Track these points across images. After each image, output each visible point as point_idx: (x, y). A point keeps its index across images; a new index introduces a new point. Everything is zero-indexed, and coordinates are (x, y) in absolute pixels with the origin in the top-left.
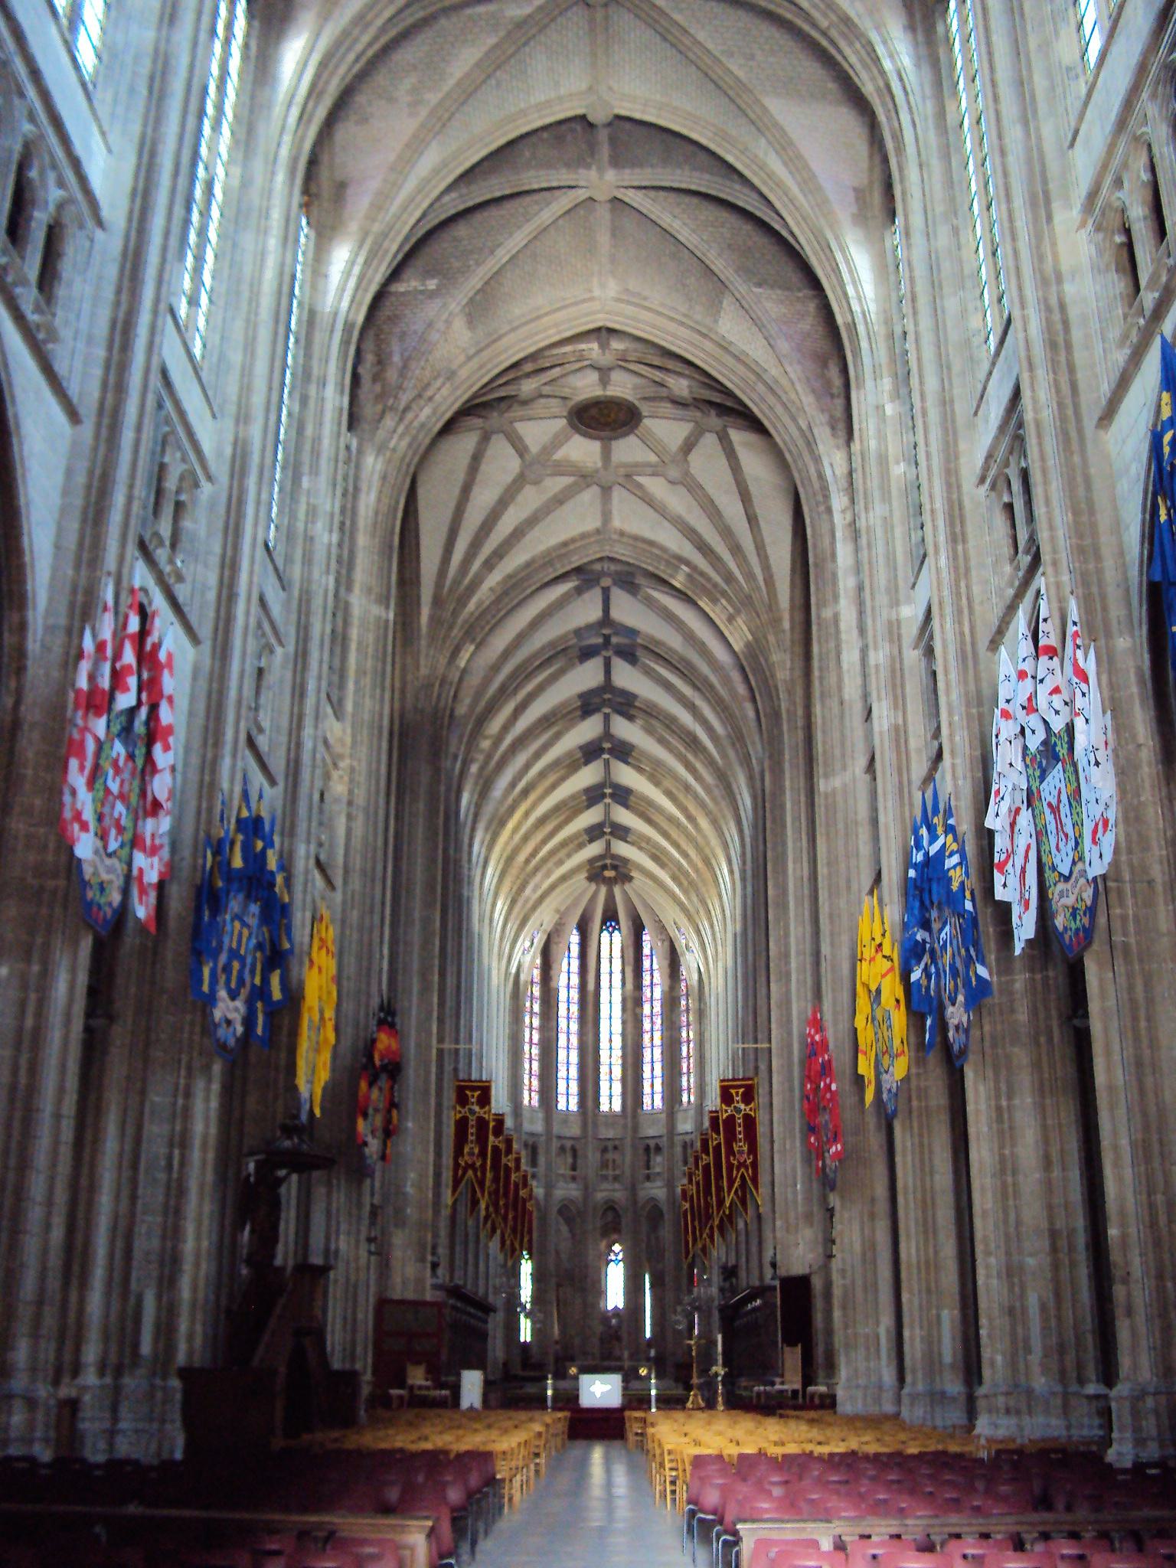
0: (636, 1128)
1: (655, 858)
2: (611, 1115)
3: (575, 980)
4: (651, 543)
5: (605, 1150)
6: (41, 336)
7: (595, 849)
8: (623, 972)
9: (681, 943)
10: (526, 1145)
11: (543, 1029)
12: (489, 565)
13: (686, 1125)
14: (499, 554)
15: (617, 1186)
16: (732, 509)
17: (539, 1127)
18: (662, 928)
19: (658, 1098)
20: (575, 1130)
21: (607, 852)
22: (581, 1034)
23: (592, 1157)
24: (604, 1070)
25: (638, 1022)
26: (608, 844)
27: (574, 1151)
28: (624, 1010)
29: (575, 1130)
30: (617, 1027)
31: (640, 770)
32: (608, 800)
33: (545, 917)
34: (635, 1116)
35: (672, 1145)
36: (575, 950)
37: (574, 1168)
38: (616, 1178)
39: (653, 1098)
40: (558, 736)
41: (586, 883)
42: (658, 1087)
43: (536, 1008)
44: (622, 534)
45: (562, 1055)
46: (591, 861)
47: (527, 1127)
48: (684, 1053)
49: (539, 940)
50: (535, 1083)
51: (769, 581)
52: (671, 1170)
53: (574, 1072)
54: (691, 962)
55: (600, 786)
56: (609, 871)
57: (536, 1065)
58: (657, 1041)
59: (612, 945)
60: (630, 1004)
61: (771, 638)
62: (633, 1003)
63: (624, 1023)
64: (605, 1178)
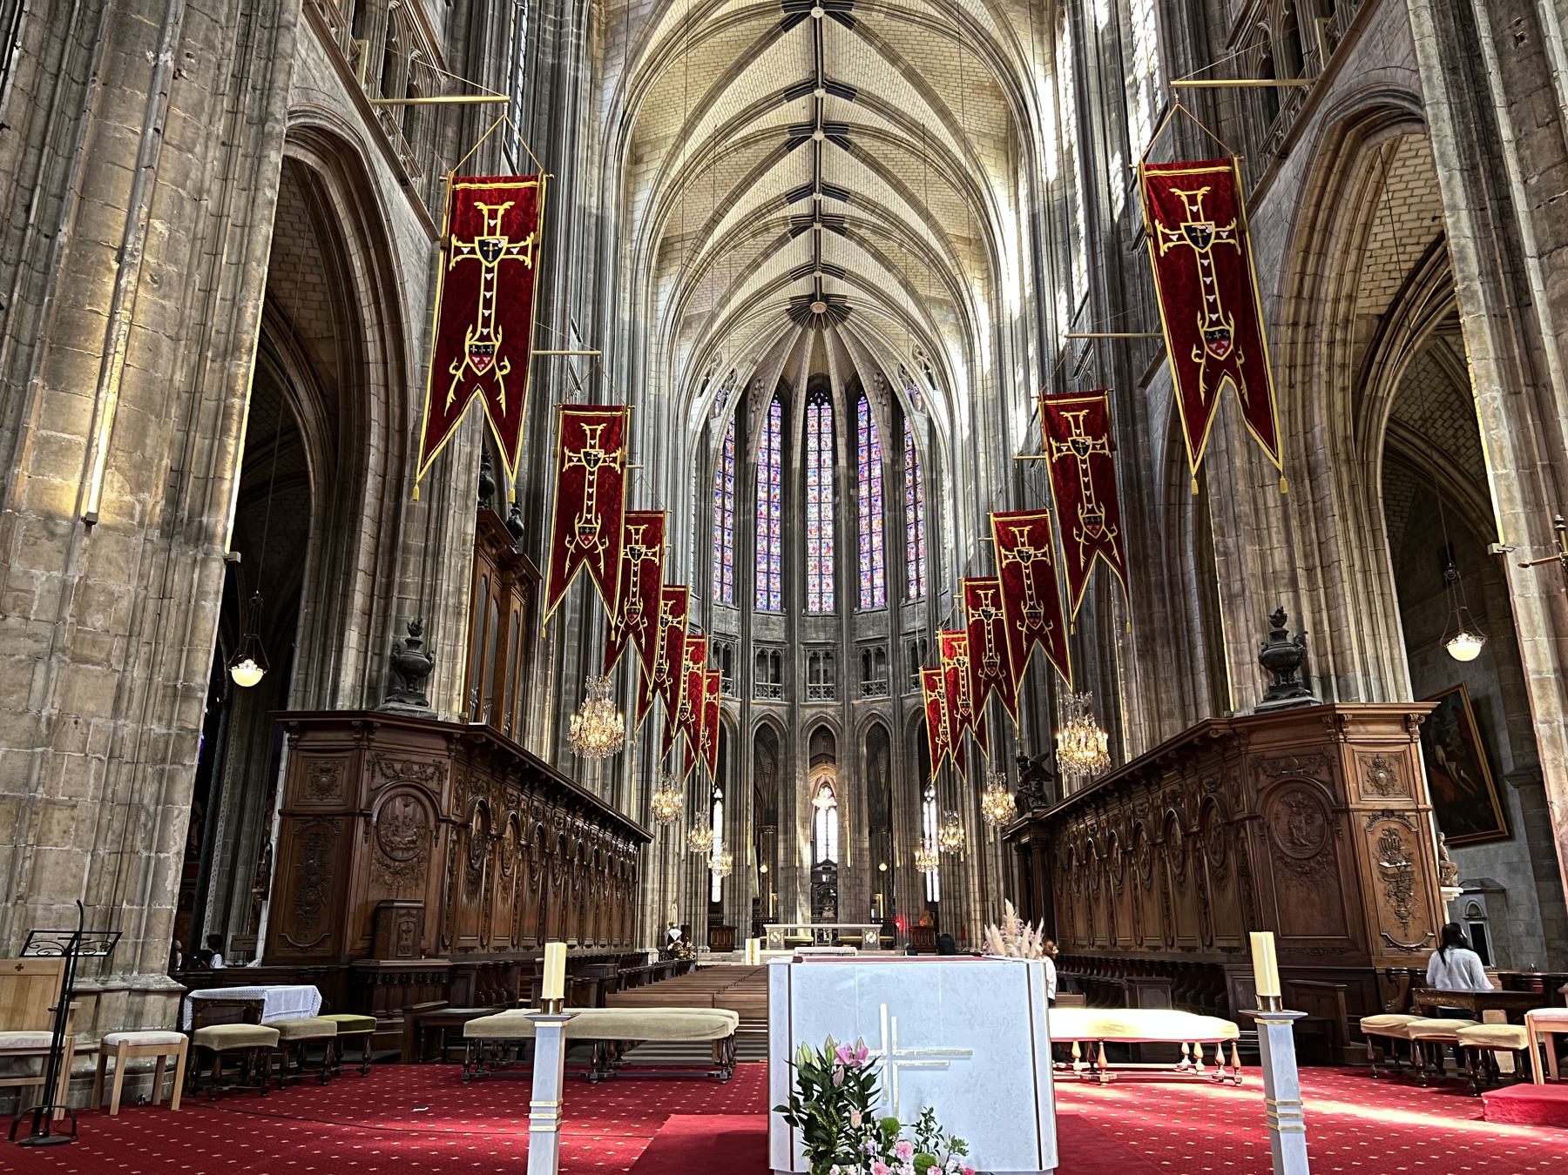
0: (852, 629)
1: (878, 256)
2: (822, 615)
3: (776, 458)
5: (814, 659)
7: (796, 253)
8: (834, 449)
9: (904, 401)
10: (716, 651)
11: (735, 513)
15: (830, 701)
17: (733, 628)
19: (878, 593)
21: (816, 265)
22: (785, 521)
23: (802, 667)
24: (812, 563)
25: (853, 504)
28: (835, 493)
29: (778, 634)
30: (828, 513)
31: (867, 34)
32: (819, 135)
33: (736, 357)
35: (896, 649)
36: (776, 422)
37: (776, 679)
38: (828, 692)
41: (786, 318)
42: (878, 581)
43: (730, 487)
45: (762, 545)
46: (796, 274)
47: (717, 625)
48: (911, 538)
49: (734, 397)
50: (728, 577)
53: (776, 566)
56: (817, 311)
57: (729, 554)
58: (877, 526)
59: (819, 423)
60: (843, 483)
62: (846, 485)
63: (835, 507)
64: (815, 692)
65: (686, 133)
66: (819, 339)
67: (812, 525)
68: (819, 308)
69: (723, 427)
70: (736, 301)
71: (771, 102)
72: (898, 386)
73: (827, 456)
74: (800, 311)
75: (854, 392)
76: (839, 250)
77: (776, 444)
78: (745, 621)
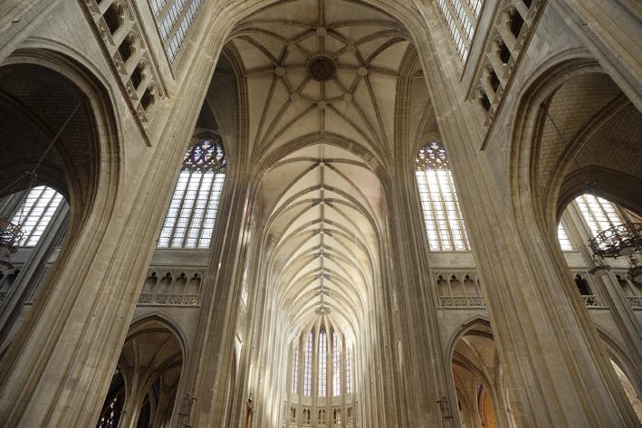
0: (331, 402)
1: (338, 302)
3: (311, 349)
4: (339, 136)
5: (320, 412)
6: (141, 118)
7: (317, 299)
9: (346, 336)
12: (276, 137)
13: (349, 401)
14: (280, 133)
16: (371, 113)
17: (297, 403)
18: (340, 330)
19: (339, 391)
20: (309, 404)
22: (313, 368)
23: (314, 415)
24: (320, 381)
25: (332, 364)
26: (322, 298)
27: (309, 411)
28: (327, 360)
30: (325, 366)
31: (334, 261)
34: (331, 398)
35: (344, 409)
38: (324, 423)
39: (337, 392)
40: (305, 241)
44: (328, 133)
45: (306, 376)
46: (317, 304)
47: (292, 401)
49: (300, 333)
50: (296, 386)
51: (385, 139)
52: (344, 417)
53: (309, 383)
54: (350, 342)
55: (320, 268)
56: (323, 310)
61: (386, 161)
62: (329, 358)
63: (327, 365)
64: (320, 423)
65: (292, 279)
66: (323, 321)
67: (320, 370)
68: (323, 310)
69: (296, 342)
70: (304, 309)
71: (311, 272)
72: (343, 329)
73: (325, 349)
74: (318, 312)
75: (332, 331)
76: (326, 299)
77: (311, 345)
78: (300, 399)
